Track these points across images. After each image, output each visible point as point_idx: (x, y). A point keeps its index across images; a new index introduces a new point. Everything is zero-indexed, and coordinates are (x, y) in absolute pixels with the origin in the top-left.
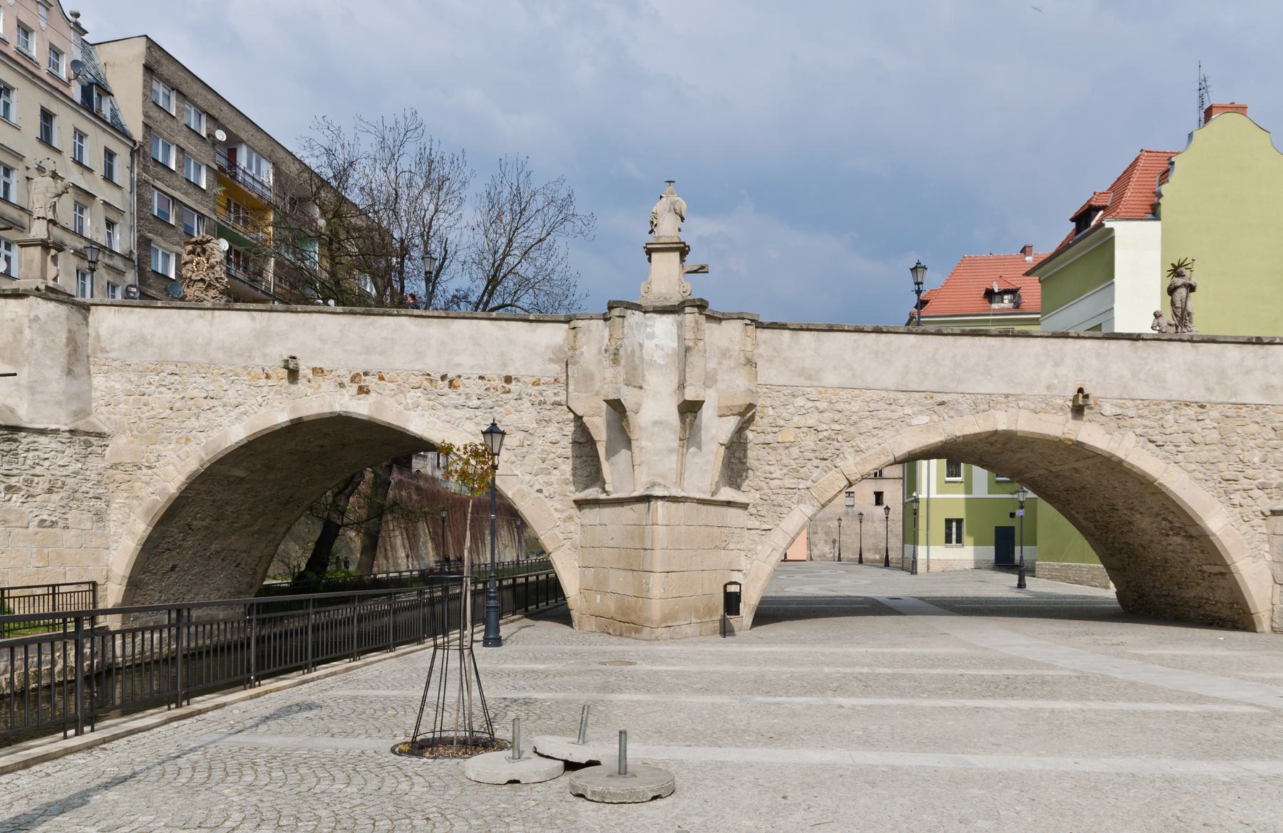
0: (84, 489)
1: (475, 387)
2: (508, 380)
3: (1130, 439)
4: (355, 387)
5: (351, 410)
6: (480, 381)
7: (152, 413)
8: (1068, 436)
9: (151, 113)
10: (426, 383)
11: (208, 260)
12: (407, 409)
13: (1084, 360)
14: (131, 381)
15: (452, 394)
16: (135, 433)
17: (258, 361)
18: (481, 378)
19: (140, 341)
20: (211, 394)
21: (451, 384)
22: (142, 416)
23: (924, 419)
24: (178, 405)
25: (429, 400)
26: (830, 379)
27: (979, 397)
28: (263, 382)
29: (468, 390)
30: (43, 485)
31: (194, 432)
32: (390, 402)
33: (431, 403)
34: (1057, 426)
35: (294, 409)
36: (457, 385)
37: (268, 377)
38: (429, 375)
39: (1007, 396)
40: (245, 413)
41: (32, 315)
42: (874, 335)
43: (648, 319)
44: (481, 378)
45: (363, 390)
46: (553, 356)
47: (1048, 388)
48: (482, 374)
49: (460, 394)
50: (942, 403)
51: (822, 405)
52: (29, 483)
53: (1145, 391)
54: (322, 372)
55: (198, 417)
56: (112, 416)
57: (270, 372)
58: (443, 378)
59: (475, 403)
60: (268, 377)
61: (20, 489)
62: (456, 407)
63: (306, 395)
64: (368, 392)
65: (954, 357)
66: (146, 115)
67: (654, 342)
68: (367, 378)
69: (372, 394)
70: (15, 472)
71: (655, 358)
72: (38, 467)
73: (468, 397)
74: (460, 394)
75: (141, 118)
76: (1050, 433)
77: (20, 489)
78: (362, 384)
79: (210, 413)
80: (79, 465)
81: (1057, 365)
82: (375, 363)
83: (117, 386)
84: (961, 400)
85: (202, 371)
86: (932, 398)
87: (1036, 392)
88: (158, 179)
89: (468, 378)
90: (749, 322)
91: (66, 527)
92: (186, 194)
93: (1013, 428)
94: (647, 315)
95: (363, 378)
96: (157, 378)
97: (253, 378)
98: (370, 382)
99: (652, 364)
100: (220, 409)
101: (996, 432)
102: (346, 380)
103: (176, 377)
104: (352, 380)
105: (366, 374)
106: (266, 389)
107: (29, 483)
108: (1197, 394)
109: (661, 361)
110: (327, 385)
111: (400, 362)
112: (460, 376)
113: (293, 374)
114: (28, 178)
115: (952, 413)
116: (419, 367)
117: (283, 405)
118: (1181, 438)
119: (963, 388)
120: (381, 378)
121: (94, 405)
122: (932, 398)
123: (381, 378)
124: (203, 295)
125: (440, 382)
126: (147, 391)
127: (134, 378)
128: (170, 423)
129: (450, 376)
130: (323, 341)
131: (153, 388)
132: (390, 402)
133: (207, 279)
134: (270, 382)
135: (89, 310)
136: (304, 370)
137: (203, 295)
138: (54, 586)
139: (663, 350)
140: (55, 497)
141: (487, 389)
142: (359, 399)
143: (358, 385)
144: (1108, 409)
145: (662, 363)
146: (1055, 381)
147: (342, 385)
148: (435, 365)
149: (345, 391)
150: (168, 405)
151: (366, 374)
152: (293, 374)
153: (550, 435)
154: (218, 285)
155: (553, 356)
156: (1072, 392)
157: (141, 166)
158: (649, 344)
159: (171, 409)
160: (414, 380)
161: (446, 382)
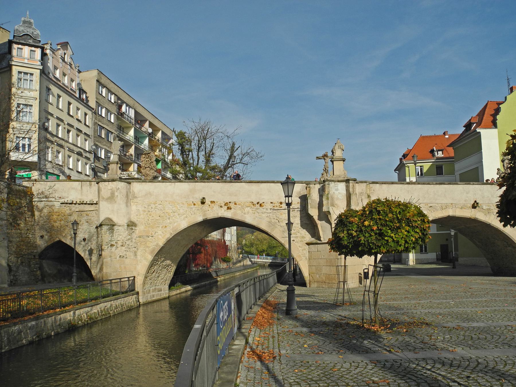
0: (131, 245)
1: (270, 206)
5: (225, 215)
6: (271, 204)
7: (153, 218)
8: (473, 216)
9: (98, 97)
10: (252, 205)
11: (150, 160)
12: (245, 214)
13: (476, 192)
14: (145, 207)
15: (261, 208)
16: (146, 225)
17: (192, 200)
18: (271, 203)
19: (149, 194)
20: (174, 211)
21: (261, 205)
22: (149, 219)
24: (162, 215)
25: (253, 211)
27: (443, 204)
28: (193, 206)
29: (267, 207)
30: (120, 243)
31: (168, 224)
32: (239, 212)
33: (253, 212)
34: (469, 213)
35: (204, 215)
36: (263, 205)
37: (194, 205)
38: (252, 202)
39: (452, 204)
40: (186, 217)
41: (117, 187)
42: (407, 185)
43: (336, 184)
44: (271, 203)
45: (229, 208)
46: (297, 195)
47: (465, 201)
48: (272, 202)
49: (264, 209)
50: (431, 207)
52: (116, 243)
54: (214, 202)
55: (169, 219)
56: (139, 219)
57: (195, 203)
58: (258, 203)
60: (194, 205)
61: (114, 245)
62: (262, 213)
63: (208, 210)
64: (231, 209)
65: (434, 192)
66: (97, 98)
67: (338, 191)
68: (230, 204)
69: (232, 209)
70: (113, 240)
71: (339, 197)
72: (119, 238)
73: (267, 209)
74: (264, 209)
75: (95, 100)
76: (467, 216)
77: (114, 245)
78: (229, 206)
79: (173, 218)
80: (130, 237)
81: (467, 193)
82: (233, 199)
83: (140, 209)
84: (437, 205)
85: (170, 203)
86: (427, 205)
87: (461, 202)
88: (100, 121)
89: (267, 203)
90: (368, 184)
91: (126, 258)
92: (108, 125)
93: (455, 214)
94: (336, 183)
95: (229, 204)
96: (154, 206)
97: (189, 205)
98: (232, 205)
99: (338, 199)
100: (177, 216)
101: (449, 216)
102: (223, 205)
103: (161, 205)
104: (225, 205)
105: (230, 203)
106: (194, 209)
107: (116, 243)
109: (340, 198)
110: (216, 207)
111: (242, 199)
112: (264, 203)
113: (203, 203)
114: (64, 128)
115: (434, 210)
117: (200, 214)
119: (437, 201)
120: (235, 204)
121: (132, 216)
122: (427, 205)
123: (235, 204)
124: (149, 173)
125: (257, 204)
126: (151, 211)
127: (146, 207)
128: (160, 221)
129: (260, 203)
130: (214, 192)
131: (153, 209)
132: (239, 212)
133: (150, 166)
134: (195, 206)
135: (130, 184)
136: (207, 201)
137: (149, 173)
138: (120, 279)
139: (341, 194)
140: (123, 248)
141: (273, 207)
142: (228, 211)
143: (227, 207)
145: (341, 198)
146: (467, 199)
147: (221, 207)
149: (222, 209)
150: (158, 215)
151: (230, 203)
152: (203, 203)
153: (296, 222)
154: (154, 169)
155: (297, 195)
156: (473, 202)
157: (95, 117)
158: (337, 192)
159: (160, 216)
160: (247, 204)
161: (259, 205)
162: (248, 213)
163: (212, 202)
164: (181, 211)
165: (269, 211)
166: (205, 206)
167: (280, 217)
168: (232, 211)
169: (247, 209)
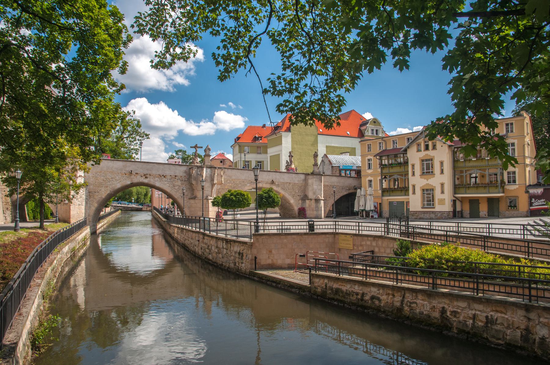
1: (169, 177)
2: (176, 176)
3: (280, 188)
4: (144, 177)
15: (164, 178)
17: (124, 171)
21: (164, 177)
23: (249, 185)
24: (105, 179)
26: (234, 178)
32: (152, 180)
35: (131, 181)
45: (146, 178)
51: (232, 182)
53: (282, 181)
59: (169, 180)
60: (126, 174)
82: (149, 172)
98: (148, 176)
104: (144, 175)
108: (289, 181)
110: (139, 177)
116: (158, 173)
118: (287, 188)
132: (152, 180)
144: (277, 184)
147: (142, 176)
148: (161, 173)
160: (157, 176)
162: (157, 181)
163: (136, 173)
164: (117, 177)
165: (169, 180)
166: (133, 176)
167: (175, 184)
168: (148, 179)
169: (156, 179)
